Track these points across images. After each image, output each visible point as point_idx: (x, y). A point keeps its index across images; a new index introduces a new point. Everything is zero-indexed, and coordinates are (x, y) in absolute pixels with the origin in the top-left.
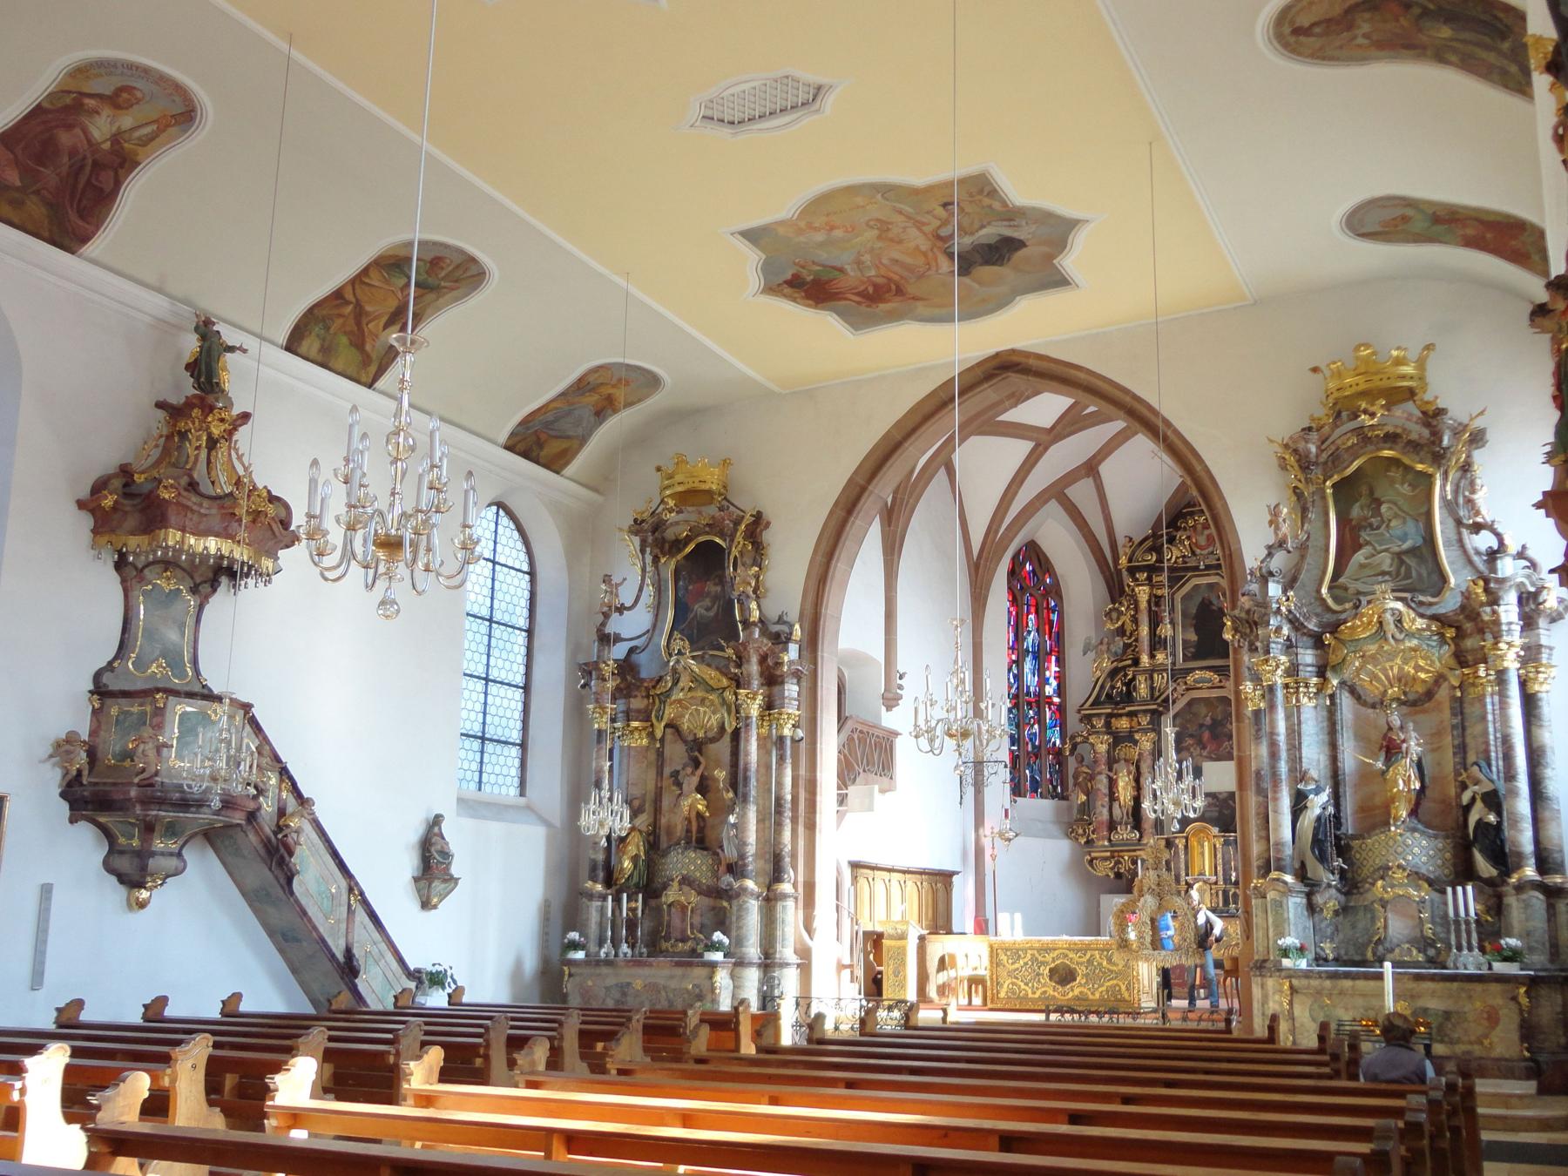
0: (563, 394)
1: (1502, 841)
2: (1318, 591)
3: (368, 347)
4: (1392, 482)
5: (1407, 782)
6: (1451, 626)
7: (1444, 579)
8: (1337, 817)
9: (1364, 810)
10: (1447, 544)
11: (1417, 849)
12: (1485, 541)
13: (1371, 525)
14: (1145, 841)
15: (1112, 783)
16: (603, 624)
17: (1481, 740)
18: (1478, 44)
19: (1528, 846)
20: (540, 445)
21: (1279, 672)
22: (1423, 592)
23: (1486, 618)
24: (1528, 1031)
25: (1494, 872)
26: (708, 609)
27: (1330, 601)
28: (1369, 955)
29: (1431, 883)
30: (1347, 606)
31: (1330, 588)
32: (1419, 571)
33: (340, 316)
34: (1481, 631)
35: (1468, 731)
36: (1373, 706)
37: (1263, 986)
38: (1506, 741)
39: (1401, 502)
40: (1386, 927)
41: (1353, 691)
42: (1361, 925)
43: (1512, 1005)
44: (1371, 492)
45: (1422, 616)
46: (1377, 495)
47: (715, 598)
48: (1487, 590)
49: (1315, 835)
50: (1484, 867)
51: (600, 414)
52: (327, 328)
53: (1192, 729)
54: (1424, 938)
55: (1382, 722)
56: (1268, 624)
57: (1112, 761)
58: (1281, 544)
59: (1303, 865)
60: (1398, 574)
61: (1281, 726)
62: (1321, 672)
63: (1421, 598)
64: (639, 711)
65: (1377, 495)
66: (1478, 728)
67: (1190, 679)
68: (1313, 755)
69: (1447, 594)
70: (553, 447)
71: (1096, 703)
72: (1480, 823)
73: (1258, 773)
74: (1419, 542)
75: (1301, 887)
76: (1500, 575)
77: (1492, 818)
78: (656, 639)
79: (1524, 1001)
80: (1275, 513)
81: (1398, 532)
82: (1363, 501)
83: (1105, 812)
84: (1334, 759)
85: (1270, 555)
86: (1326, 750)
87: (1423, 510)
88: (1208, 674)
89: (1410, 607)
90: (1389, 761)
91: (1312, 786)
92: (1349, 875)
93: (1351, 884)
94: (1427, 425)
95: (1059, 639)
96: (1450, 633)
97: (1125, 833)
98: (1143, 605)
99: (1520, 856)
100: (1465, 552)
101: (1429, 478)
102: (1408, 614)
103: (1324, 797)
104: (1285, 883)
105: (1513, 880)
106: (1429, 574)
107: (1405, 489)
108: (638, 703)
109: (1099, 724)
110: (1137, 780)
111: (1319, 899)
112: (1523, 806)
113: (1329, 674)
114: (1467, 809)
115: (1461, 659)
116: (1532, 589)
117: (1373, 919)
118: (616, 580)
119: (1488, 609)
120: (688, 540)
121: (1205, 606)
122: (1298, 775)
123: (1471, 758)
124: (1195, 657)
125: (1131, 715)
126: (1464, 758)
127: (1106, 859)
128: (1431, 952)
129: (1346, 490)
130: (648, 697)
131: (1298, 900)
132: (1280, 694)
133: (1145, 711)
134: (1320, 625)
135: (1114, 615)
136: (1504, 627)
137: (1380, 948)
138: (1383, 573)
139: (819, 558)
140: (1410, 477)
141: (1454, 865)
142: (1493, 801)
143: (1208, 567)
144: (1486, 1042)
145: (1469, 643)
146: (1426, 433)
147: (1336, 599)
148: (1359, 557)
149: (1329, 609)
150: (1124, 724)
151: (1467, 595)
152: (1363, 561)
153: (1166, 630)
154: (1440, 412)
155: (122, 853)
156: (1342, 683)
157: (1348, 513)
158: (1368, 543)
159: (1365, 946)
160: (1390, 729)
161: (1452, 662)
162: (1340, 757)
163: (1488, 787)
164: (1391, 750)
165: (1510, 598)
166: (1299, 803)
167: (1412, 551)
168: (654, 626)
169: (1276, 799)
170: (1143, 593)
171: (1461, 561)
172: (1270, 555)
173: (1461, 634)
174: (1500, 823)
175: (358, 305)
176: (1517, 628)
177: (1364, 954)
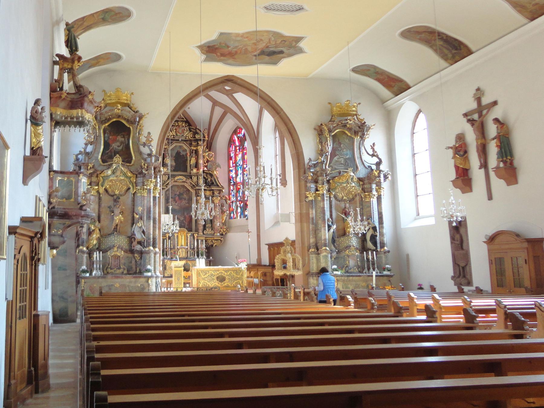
7: (357, 168)
10: (358, 158)
14: (215, 234)
36: (340, 201)
64: (94, 182)
67: (176, 178)
73: (313, 218)
74: (351, 156)
88: (181, 177)
101: (353, 139)
121: (178, 153)
124: (174, 171)
138: (342, 164)
143: (182, 140)
148: (336, 158)
160: (345, 208)
167: (349, 158)
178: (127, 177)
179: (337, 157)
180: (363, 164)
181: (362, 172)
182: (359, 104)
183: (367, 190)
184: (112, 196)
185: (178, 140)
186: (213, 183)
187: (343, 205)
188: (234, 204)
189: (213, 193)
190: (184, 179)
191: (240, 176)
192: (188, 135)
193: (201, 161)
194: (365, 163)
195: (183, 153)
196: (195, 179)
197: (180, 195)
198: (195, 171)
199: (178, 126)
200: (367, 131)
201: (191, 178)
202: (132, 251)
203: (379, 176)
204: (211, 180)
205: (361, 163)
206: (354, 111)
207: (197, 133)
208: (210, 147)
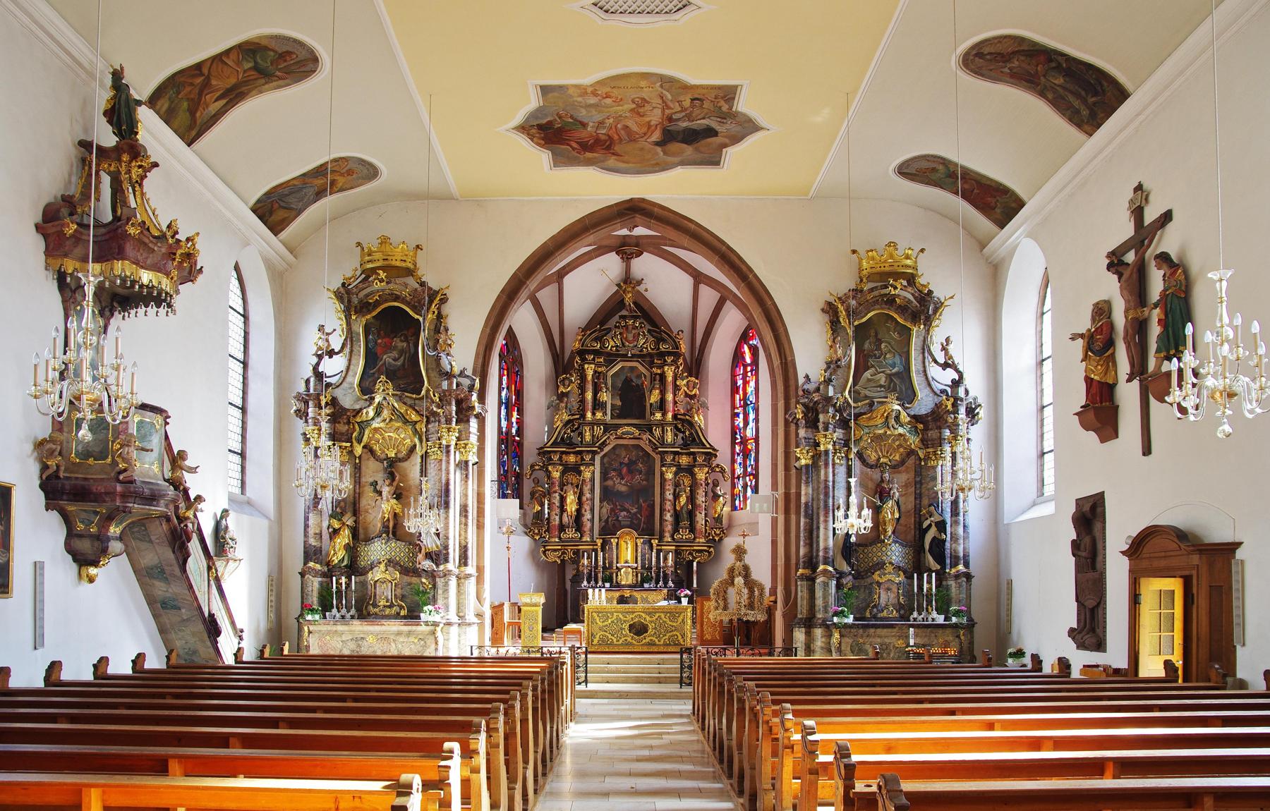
0: (304, 175)
3: (198, 114)
4: (889, 330)
5: (893, 514)
15: (563, 500)
16: (318, 364)
18: (1071, 92)
20: (271, 213)
26: (395, 360)
32: (903, 387)
33: (192, 84)
36: (871, 467)
44: (876, 334)
47: (402, 352)
50: (935, 566)
51: (320, 194)
52: (178, 93)
53: (616, 465)
57: (562, 485)
67: (619, 432)
70: (280, 214)
71: (555, 444)
78: (349, 379)
82: (872, 339)
83: (557, 518)
88: (627, 429)
95: (519, 393)
96: (921, 426)
97: (571, 534)
98: (590, 378)
100: (927, 378)
102: (903, 414)
107: (896, 336)
108: (342, 428)
109: (556, 458)
110: (580, 498)
111: (844, 581)
115: (925, 443)
118: (328, 330)
120: (377, 304)
121: (627, 381)
124: (619, 417)
125: (580, 453)
127: (555, 550)
129: (862, 333)
130: (349, 423)
133: (588, 452)
135: (567, 382)
138: (881, 386)
139: (488, 330)
143: (633, 356)
145: (932, 434)
148: (867, 374)
150: (572, 459)
153: (605, 397)
155: (80, 536)
160: (882, 481)
163: (936, 518)
168: (348, 369)
170: (590, 370)
173: (926, 429)
175: (208, 78)
178: (406, 422)
179: (871, 371)
180: (929, 385)
181: (924, 403)
182: (922, 250)
183: (932, 444)
184: (381, 461)
185: (626, 355)
186: (694, 440)
187: (876, 475)
188: (741, 482)
189: (695, 460)
190: (637, 432)
191: (752, 425)
192: (644, 342)
193: (670, 397)
194: (933, 384)
195: (636, 381)
196: (657, 432)
197: (631, 463)
198: (658, 416)
199: (626, 327)
200: (936, 310)
201: (651, 431)
202: (414, 571)
203: (956, 412)
204: (691, 434)
205: (924, 384)
206: (908, 267)
207: (664, 341)
208: (696, 367)
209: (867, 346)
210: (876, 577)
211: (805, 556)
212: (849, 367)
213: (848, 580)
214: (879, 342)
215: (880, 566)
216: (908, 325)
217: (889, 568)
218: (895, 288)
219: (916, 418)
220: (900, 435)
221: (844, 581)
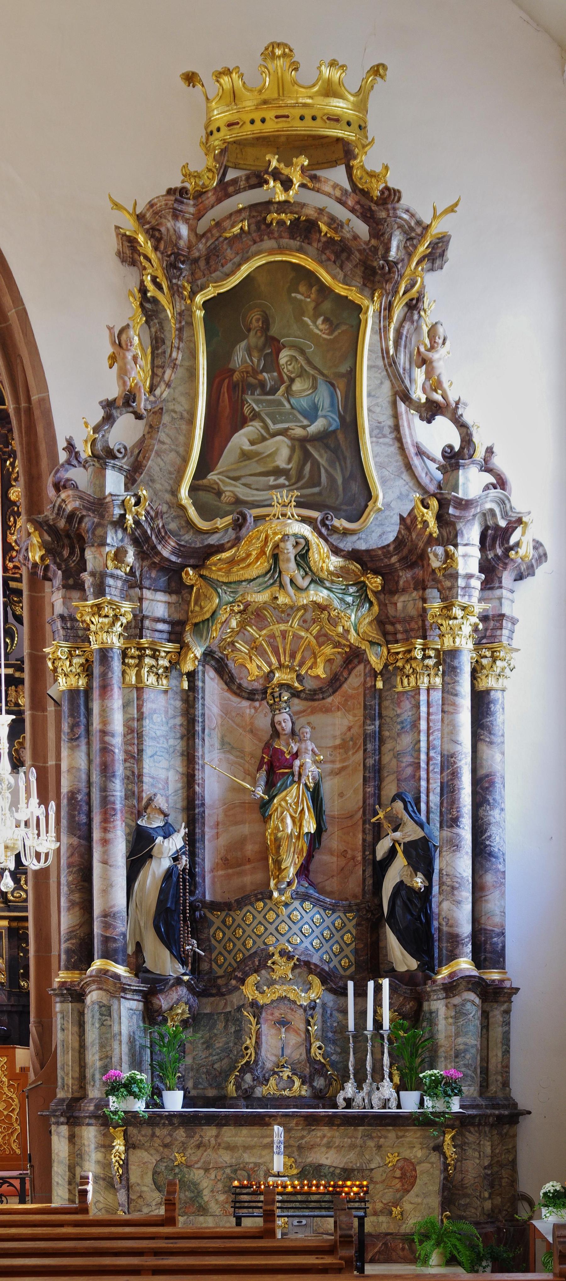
1: (429, 918)
2: (175, 492)
4: (300, 311)
5: (298, 822)
6: (376, 572)
7: (369, 495)
8: (191, 872)
9: (230, 861)
11: (304, 927)
12: (438, 435)
13: (262, 384)
17: (408, 759)
19: (465, 929)
21: (118, 628)
22: (338, 512)
23: (435, 564)
24: (451, 1194)
25: (413, 964)
27: (192, 512)
28: (231, 1088)
29: (326, 978)
30: (220, 523)
31: (193, 489)
32: (331, 476)
34: (421, 586)
35: (388, 746)
36: (251, 696)
37: (72, 1138)
38: (449, 763)
39: (311, 350)
40: (258, 1045)
41: (222, 669)
42: (219, 1044)
43: (435, 1157)
45: (336, 551)
46: (274, 331)
48: (441, 518)
49: (161, 902)
50: (402, 959)
54: (311, 1061)
55: (263, 722)
56: (103, 543)
58: (129, 399)
59: (139, 947)
60: (300, 476)
61: (117, 724)
62: (176, 633)
63: (337, 523)
65: (274, 331)
66: (406, 740)
68: (161, 773)
69: (370, 517)
72: (400, 886)
74: (335, 424)
75: (135, 984)
76: (460, 495)
77: (419, 882)
79: (449, 1150)
80: (120, 342)
81: (304, 403)
82: (254, 339)
84: (190, 779)
85: (109, 419)
86: (178, 764)
87: (344, 368)
89: (321, 535)
90: (272, 786)
91: (158, 823)
92: (205, 966)
93: (208, 984)
94: (367, 216)
99: (454, 939)
100: (402, 448)
103: (177, 842)
104: (117, 977)
105: (445, 972)
106: (345, 481)
107: (319, 327)
111: (163, 1002)
112: (464, 865)
113: (188, 638)
114: (380, 868)
115: (387, 628)
116: (503, 523)
117: (239, 1035)
119: (440, 550)
122: (139, 806)
123: (390, 789)
126: (379, 788)
128: (320, 1083)
131: (134, 1004)
132: (116, 665)
134: (179, 551)
136: (461, 582)
137: (248, 1077)
138: (277, 472)
140: (327, 306)
141: (356, 952)
142: (421, 855)
144: (396, 1211)
145: (405, 604)
146: (362, 229)
147: (206, 512)
148: (241, 439)
149: (190, 524)
151: (408, 523)
152: (247, 447)
154: (390, 196)
156: (208, 654)
157: (229, 355)
158: (256, 416)
159: (225, 1075)
160: (276, 733)
161: (375, 635)
162: (198, 775)
163: (410, 832)
164: (275, 768)
165: (471, 534)
166: (140, 849)
167: (322, 438)
169: (105, 842)
171: (397, 462)
172: (109, 419)
173: (390, 589)
174: (429, 889)
176: (476, 583)
177: (221, 1087)
179: (251, 429)
180: (409, 467)
209: (240, 357)
210: (249, 991)
211: (71, 935)
212: (191, 421)
213: (176, 1002)
214: (273, 345)
215: (259, 961)
216: (353, 294)
217: (283, 968)
218: (287, 184)
219: (364, 560)
220: (321, 608)
221: (163, 1002)
